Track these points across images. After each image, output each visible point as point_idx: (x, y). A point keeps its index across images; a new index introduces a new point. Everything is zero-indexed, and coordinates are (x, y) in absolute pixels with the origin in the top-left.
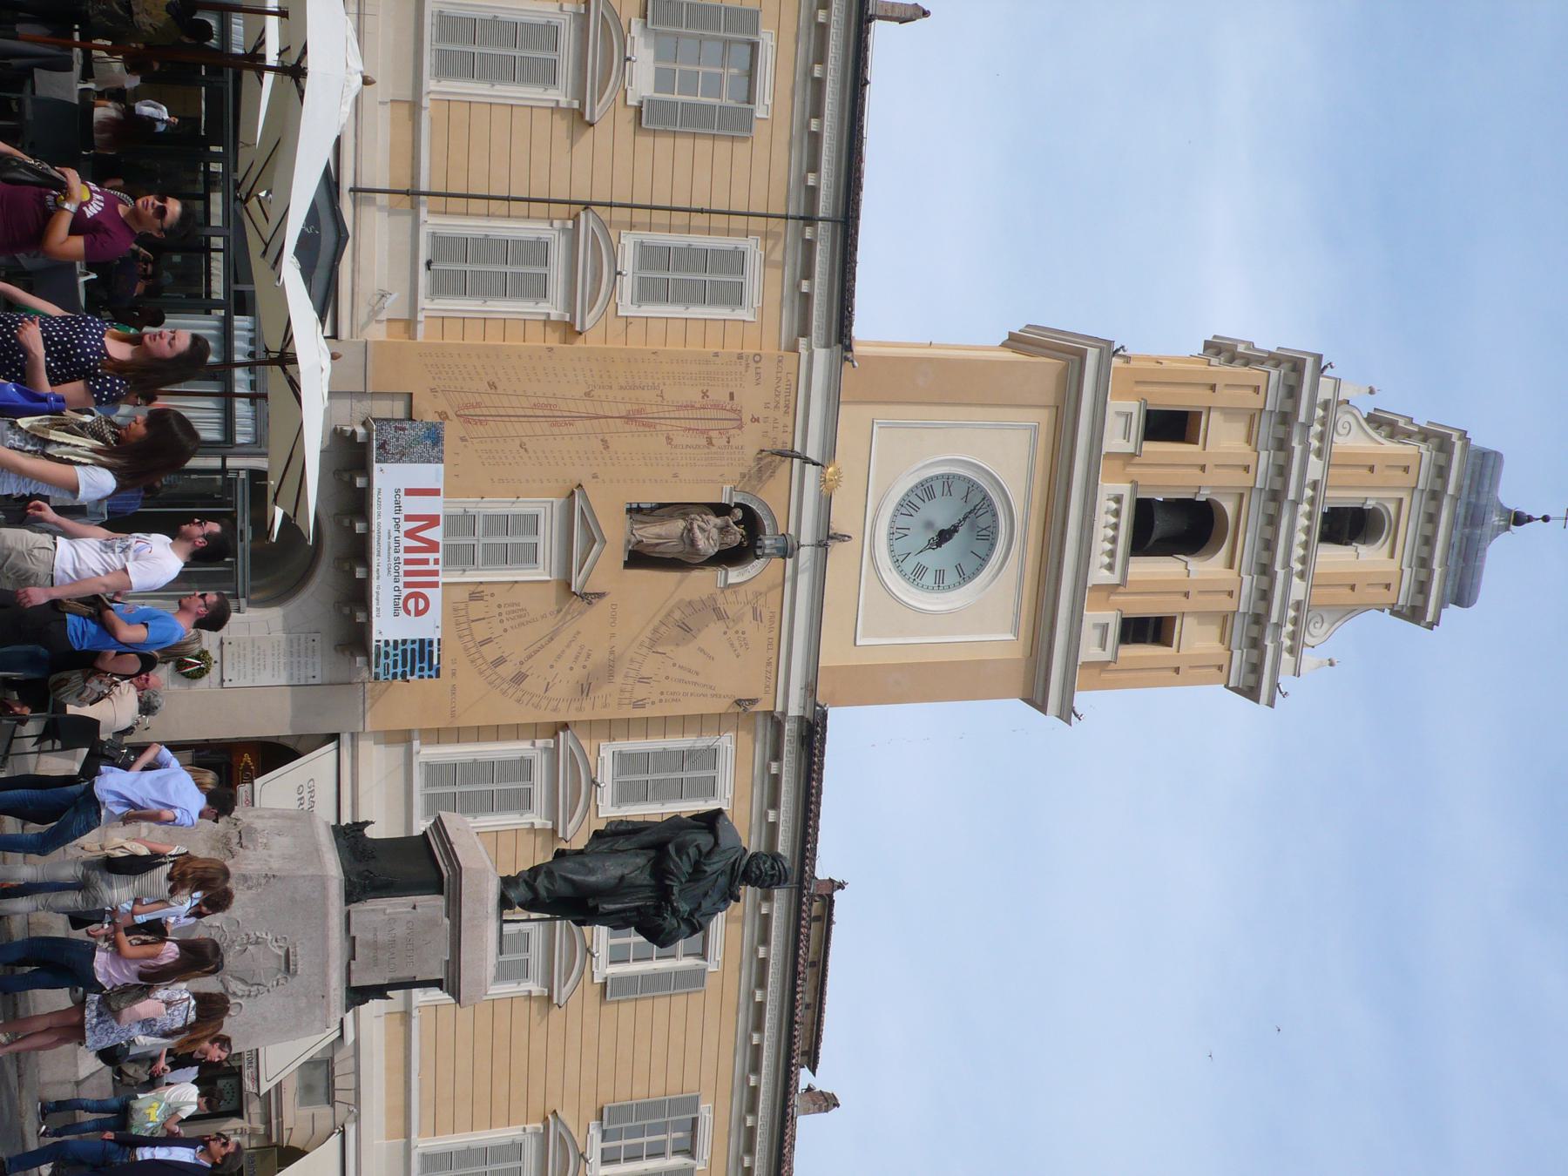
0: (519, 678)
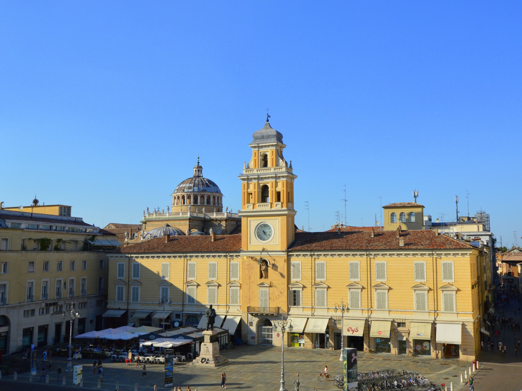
0: (281, 293)
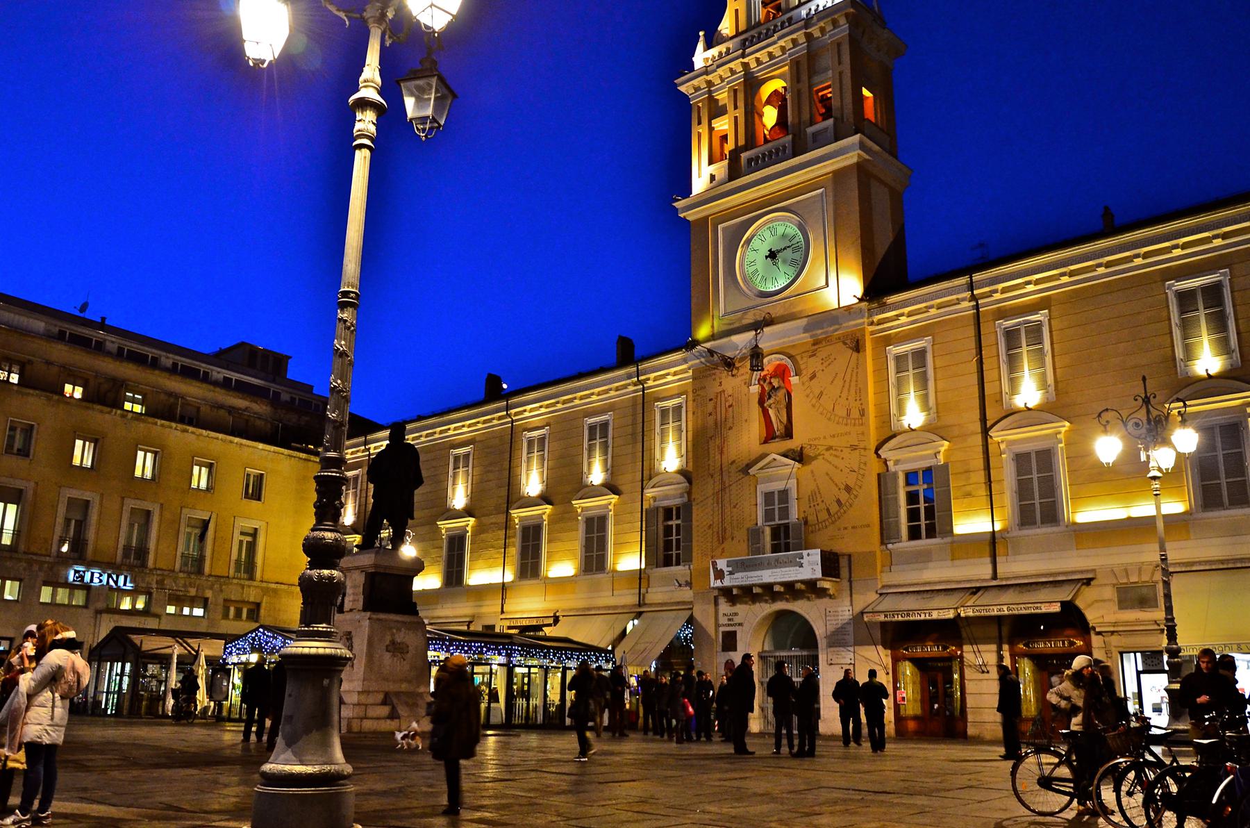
0: (848, 489)
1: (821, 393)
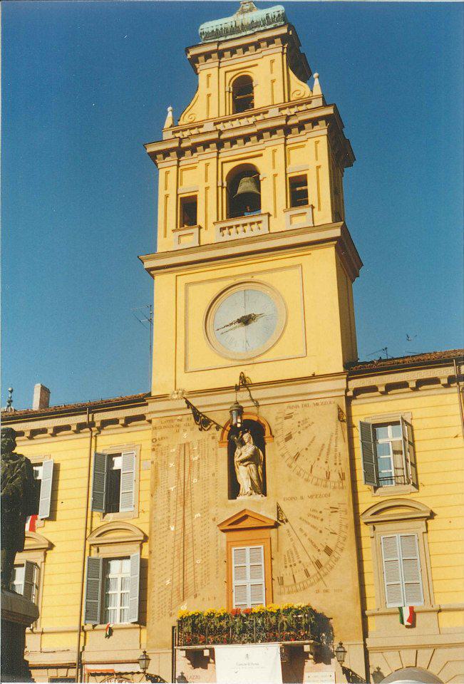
0: (328, 551)
1: (298, 455)
